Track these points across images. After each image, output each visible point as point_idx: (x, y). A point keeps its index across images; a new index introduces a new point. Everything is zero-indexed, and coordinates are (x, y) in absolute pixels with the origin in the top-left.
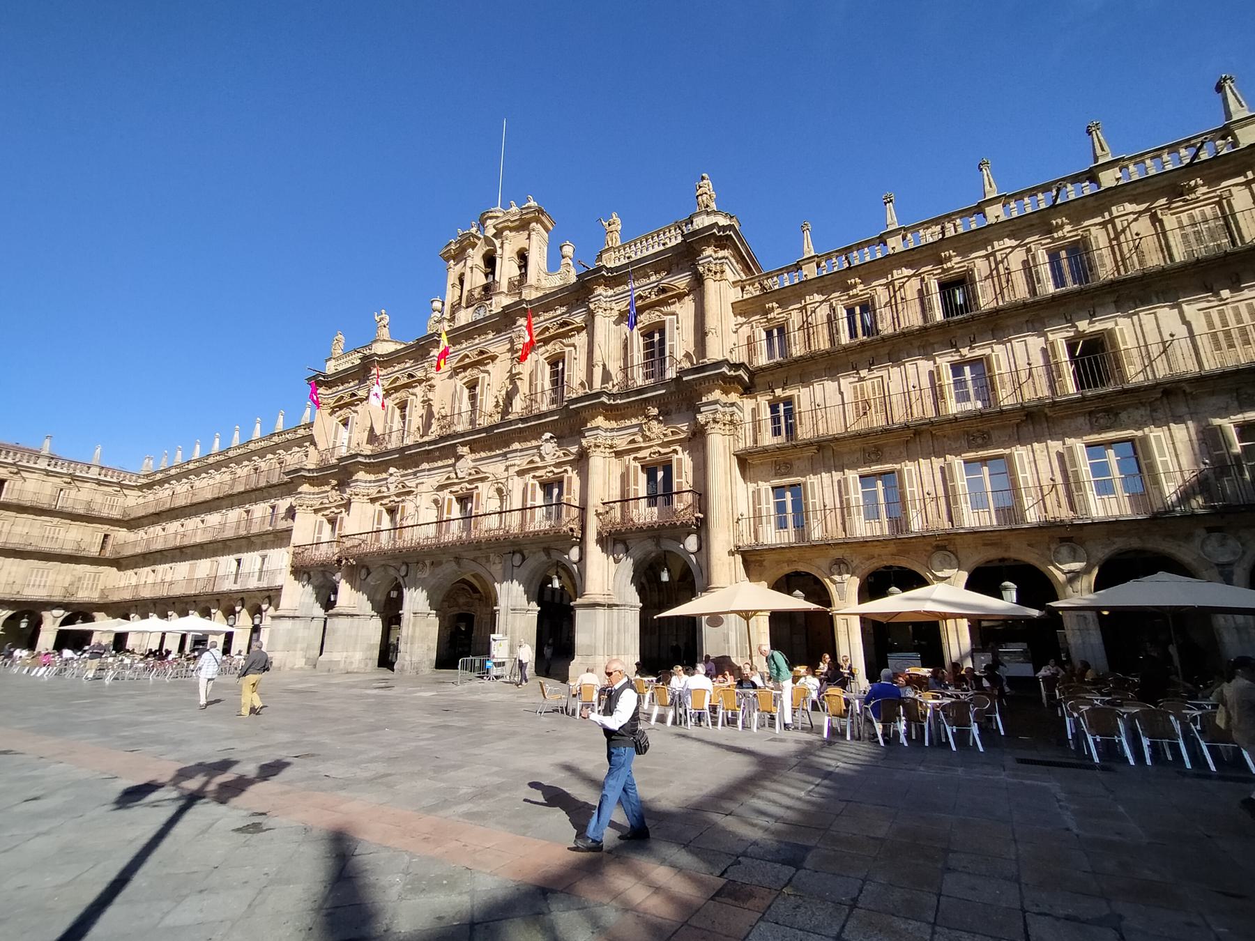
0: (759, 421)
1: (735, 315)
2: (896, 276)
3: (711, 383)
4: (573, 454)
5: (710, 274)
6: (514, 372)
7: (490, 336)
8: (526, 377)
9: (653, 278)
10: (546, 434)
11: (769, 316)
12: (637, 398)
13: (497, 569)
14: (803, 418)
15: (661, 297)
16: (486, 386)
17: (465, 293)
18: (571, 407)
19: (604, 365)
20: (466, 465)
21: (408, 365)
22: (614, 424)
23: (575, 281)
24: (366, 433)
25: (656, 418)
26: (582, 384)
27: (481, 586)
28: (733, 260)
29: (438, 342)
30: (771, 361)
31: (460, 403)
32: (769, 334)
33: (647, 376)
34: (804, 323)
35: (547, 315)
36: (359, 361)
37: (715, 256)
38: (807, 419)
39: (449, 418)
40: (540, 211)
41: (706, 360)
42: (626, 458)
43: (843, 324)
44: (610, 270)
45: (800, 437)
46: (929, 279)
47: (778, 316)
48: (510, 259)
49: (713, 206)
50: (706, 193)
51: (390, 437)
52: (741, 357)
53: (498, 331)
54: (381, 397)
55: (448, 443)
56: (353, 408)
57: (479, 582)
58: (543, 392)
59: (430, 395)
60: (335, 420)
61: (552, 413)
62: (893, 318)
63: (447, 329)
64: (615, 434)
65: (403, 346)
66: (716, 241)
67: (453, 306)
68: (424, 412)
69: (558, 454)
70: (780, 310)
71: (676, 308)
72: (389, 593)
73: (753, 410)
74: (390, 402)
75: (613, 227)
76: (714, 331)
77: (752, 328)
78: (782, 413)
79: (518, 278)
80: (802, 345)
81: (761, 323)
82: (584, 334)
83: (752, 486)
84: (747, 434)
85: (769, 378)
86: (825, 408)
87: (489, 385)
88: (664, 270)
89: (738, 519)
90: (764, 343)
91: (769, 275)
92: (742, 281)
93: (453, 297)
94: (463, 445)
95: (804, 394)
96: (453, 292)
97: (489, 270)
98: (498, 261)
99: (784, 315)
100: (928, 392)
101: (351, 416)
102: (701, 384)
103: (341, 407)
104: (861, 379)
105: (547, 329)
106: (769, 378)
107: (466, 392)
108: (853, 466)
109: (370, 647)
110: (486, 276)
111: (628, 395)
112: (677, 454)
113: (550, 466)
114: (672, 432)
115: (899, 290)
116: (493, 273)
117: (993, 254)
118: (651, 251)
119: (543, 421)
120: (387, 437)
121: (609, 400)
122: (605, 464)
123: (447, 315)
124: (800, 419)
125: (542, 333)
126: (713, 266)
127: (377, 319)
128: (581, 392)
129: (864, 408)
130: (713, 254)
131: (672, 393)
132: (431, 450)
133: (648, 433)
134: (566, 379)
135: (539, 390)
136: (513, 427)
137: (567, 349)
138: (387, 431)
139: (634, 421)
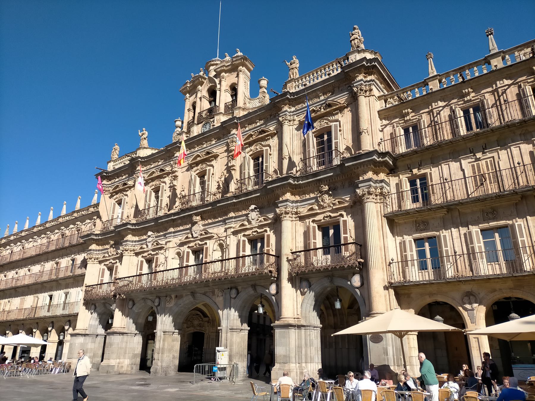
0: (402, 192)
1: (381, 120)
2: (499, 86)
3: (365, 167)
4: (270, 219)
5: (362, 93)
6: (229, 165)
7: (214, 142)
8: (237, 168)
9: (322, 98)
10: (251, 206)
11: (406, 119)
12: (313, 179)
13: (220, 300)
14: (435, 189)
15: (328, 110)
17: (197, 115)
18: (268, 187)
19: (290, 158)
20: (198, 229)
21: (160, 163)
22: (298, 198)
23: (269, 102)
24: (133, 209)
25: (327, 192)
26: (275, 171)
27: (209, 312)
28: (378, 82)
29: (180, 147)
30: (409, 150)
31: (194, 187)
32: (406, 131)
33: (319, 164)
34: (431, 122)
35: (251, 127)
36: (128, 162)
37: (365, 80)
38: (438, 190)
39: (187, 198)
40: (244, 58)
41: (361, 151)
42: (307, 221)
43: (461, 122)
45: (433, 202)
47: (412, 118)
48: (226, 91)
49: (362, 46)
50: (357, 38)
51: (148, 211)
52: (386, 148)
53: (219, 139)
54: (143, 185)
55: (187, 214)
56: (124, 193)
57: (208, 310)
58: (249, 178)
59: (175, 183)
60: (113, 201)
61: (255, 192)
63: (185, 138)
64: (299, 204)
65: (157, 151)
66: (365, 70)
67: (189, 123)
68: (170, 193)
69: (260, 219)
70: (413, 114)
71: (339, 117)
72: (147, 318)
73: (397, 185)
74: (148, 188)
75: (294, 66)
76: (366, 131)
77: (394, 127)
78: (419, 186)
79: (231, 103)
80: (431, 137)
81: (400, 124)
83: (399, 239)
84: (394, 202)
85: (408, 162)
86: (451, 181)
87: (213, 174)
88: (329, 92)
89: (390, 263)
90: (403, 138)
91: (404, 91)
92: (385, 96)
93: (189, 118)
94: (197, 214)
95: (435, 172)
96: (189, 114)
97: (212, 99)
98: (218, 92)
99: (417, 117)
101: (123, 198)
102: (358, 168)
103: (117, 193)
104: (478, 160)
105: (251, 136)
107: (198, 179)
109: (135, 356)
110: (210, 103)
111: (307, 177)
112: (343, 217)
113: (255, 227)
114: (338, 202)
115: (502, 94)
116: (215, 100)
118: (320, 80)
119: (250, 197)
120: (146, 211)
121: (294, 182)
122: (292, 226)
123: (185, 129)
124: (433, 190)
125: (248, 138)
126: (364, 87)
127: (140, 134)
128: (275, 177)
129: (481, 180)
130: (364, 78)
131: (338, 176)
132: (175, 219)
133: (322, 203)
134: (264, 168)
135: (247, 176)
136: (230, 202)
137: (264, 148)
138: (147, 207)
139: (312, 195)
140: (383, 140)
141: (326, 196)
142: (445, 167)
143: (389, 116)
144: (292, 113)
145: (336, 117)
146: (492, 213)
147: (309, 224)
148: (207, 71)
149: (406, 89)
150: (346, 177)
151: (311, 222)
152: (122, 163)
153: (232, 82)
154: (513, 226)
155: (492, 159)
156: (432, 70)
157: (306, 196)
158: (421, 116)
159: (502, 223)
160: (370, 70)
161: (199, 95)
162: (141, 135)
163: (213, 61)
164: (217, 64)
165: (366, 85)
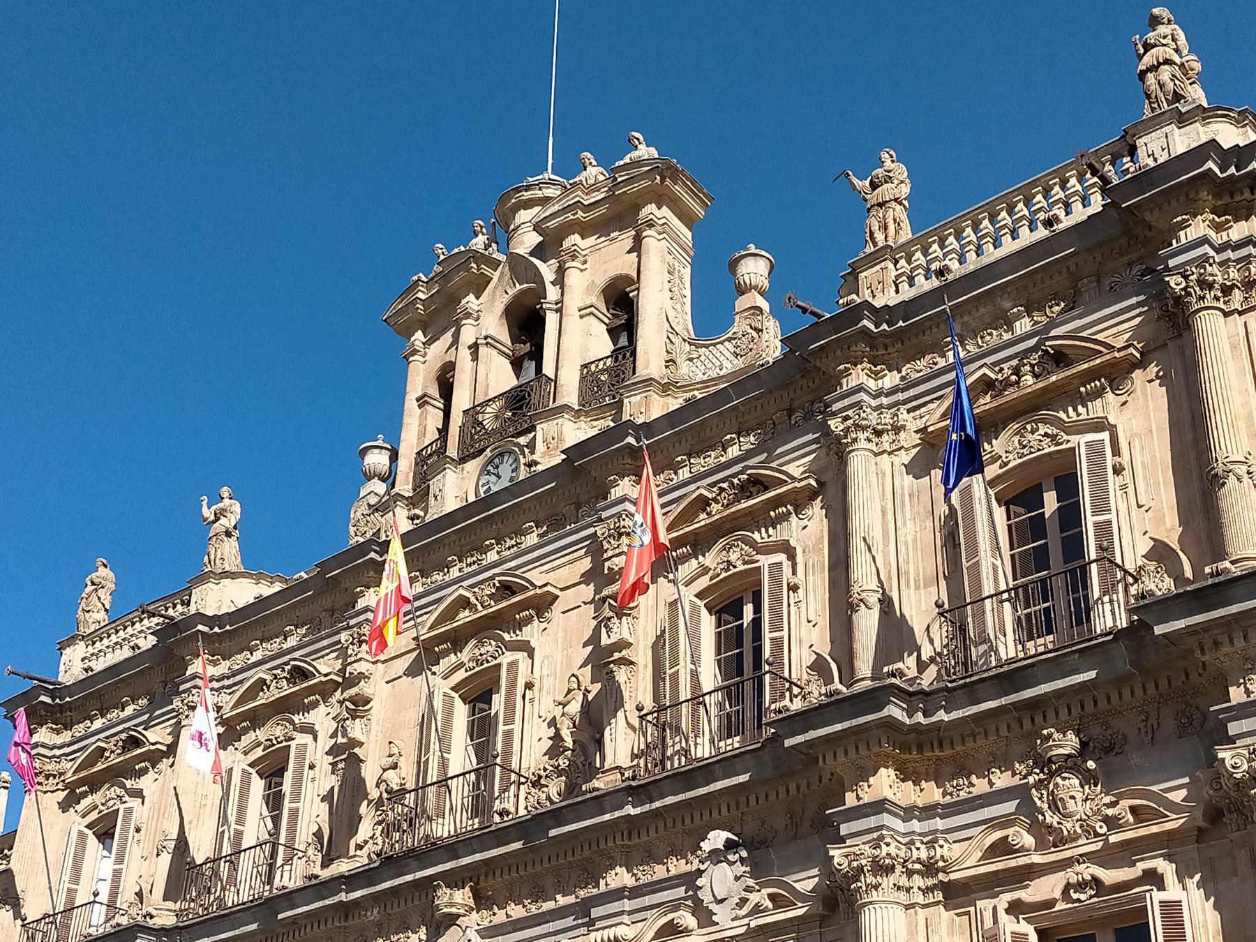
4: (803, 897)
6: (605, 640)
7: (532, 539)
8: (642, 655)
9: (1023, 326)
10: (711, 835)
12: (1003, 701)
15: (1054, 378)
16: (520, 689)
17: (457, 419)
18: (788, 743)
19: (886, 603)
21: (292, 642)
22: (932, 793)
23: (778, 353)
24: (166, 859)
25: (1072, 764)
26: (819, 667)
29: (379, 567)
31: (445, 748)
33: (1028, 630)
35: (701, 464)
36: (152, 640)
37: (1218, 238)
39: (410, 799)
40: (664, 170)
42: (985, 905)
44: (887, 314)
48: (586, 311)
49: (1197, 95)
50: (1168, 62)
51: (234, 866)
53: (555, 523)
54: (213, 744)
55: (409, 878)
56: (129, 784)
58: (697, 698)
59: (356, 729)
60: (76, 822)
61: (725, 764)
63: (405, 526)
65: (278, 587)
66: (1217, 196)
67: (421, 459)
68: (333, 781)
69: (754, 898)
71: (1108, 406)
74: (236, 760)
75: (886, 191)
79: (609, 362)
82: (816, 512)
87: (529, 686)
88: (1056, 297)
93: (423, 433)
94: (454, 880)
96: (423, 418)
97: (526, 348)
98: (551, 320)
101: (122, 807)
102: (1217, 644)
103: (94, 784)
107: (461, 712)
110: (517, 365)
111: (972, 692)
112: (1162, 887)
114: (1133, 810)
116: (537, 355)
118: (1009, 246)
119: (703, 791)
120: (224, 868)
121: (910, 717)
123: (404, 486)
125: (687, 516)
126: (1215, 269)
127: (208, 513)
128: (817, 692)
130: (1212, 234)
131: (1120, 681)
132: (355, 902)
134: (767, 653)
135: (685, 693)
136: (607, 817)
137: (765, 561)
138: (226, 850)
139: (1002, 780)
141: (1069, 784)
144: (887, 395)
145: (1096, 409)
147: (995, 921)
148: (502, 231)
150: (1163, 683)
151: (1001, 913)
152: (126, 648)
153: (613, 272)
157: (973, 785)
160: (1238, 198)
161: (469, 334)
162: (212, 518)
163: (528, 188)
164: (545, 201)
165: (1224, 264)
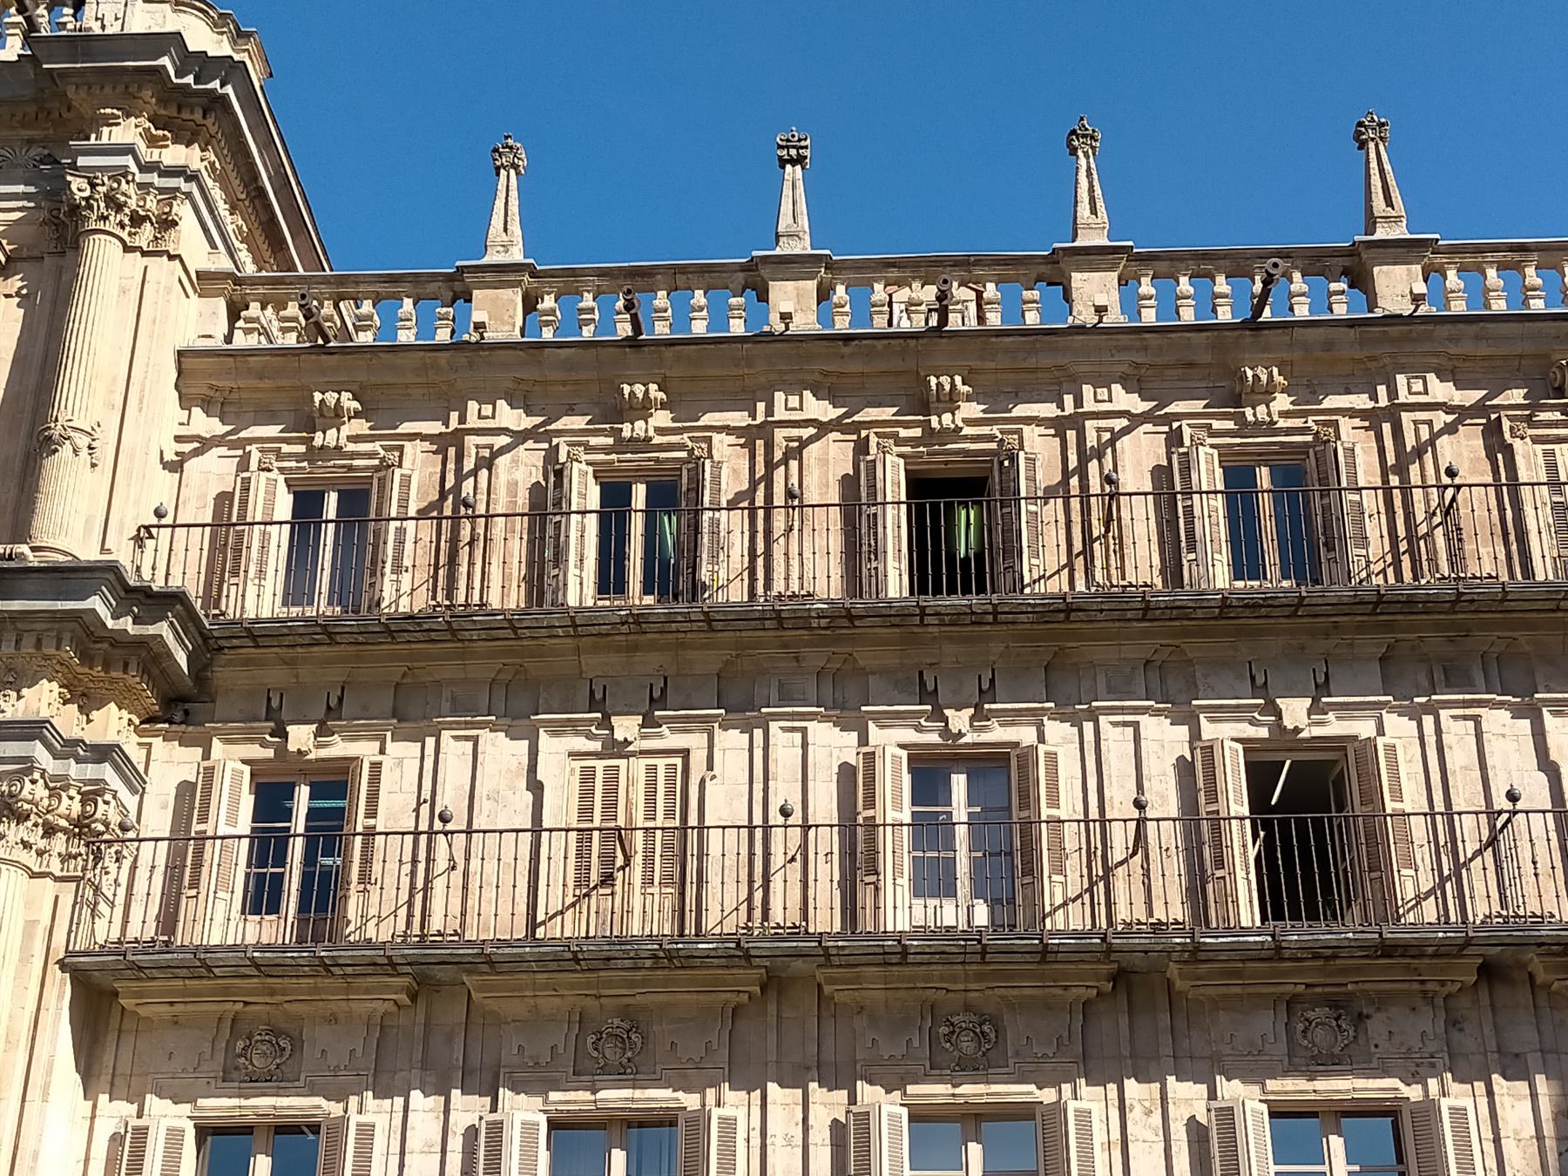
0: (202, 838)
1: (186, 402)
3: (28, 648)
5: (114, 218)
11: (318, 439)
14: (378, 856)
28: (217, 194)
30: (295, 611)
32: (307, 505)
34: (443, 495)
38: (392, 866)
45: (352, 932)
46: (884, 451)
47: (351, 447)
52: (176, 571)
62: (753, 556)
70: (361, 426)
73: (185, 789)
77: (243, 465)
78: (299, 824)
80: (422, 575)
81: (280, 456)
83: (115, 1113)
84: (140, 886)
85: (277, 676)
90: (280, 537)
91: (344, 288)
92: (238, 281)
95: (400, 762)
99: (376, 446)
100: (827, 841)
104: (615, 749)
106: (277, 676)
108: (534, 1081)
117: (1077, 421)
124: (366, 861)
126: (131, 190)
129: (607, 859)
130: (142, 146)
140: (168, 520)
142: (454, 750)
143: (234, 396)
146: (623, 1041)
149: (357, 283)
154: (699, 1121)
155: (678, 761)
156: (506, 230)
158: (401, 449)
159: (659, 1096)
160: (186, 115)
165: (144, 187)
